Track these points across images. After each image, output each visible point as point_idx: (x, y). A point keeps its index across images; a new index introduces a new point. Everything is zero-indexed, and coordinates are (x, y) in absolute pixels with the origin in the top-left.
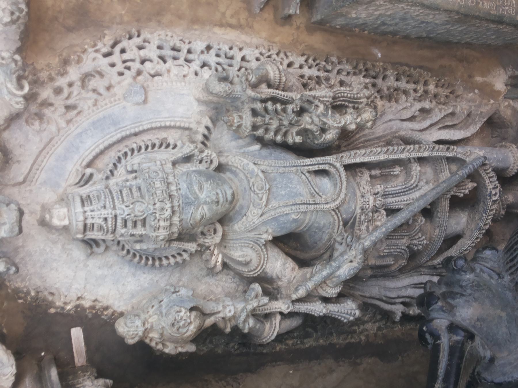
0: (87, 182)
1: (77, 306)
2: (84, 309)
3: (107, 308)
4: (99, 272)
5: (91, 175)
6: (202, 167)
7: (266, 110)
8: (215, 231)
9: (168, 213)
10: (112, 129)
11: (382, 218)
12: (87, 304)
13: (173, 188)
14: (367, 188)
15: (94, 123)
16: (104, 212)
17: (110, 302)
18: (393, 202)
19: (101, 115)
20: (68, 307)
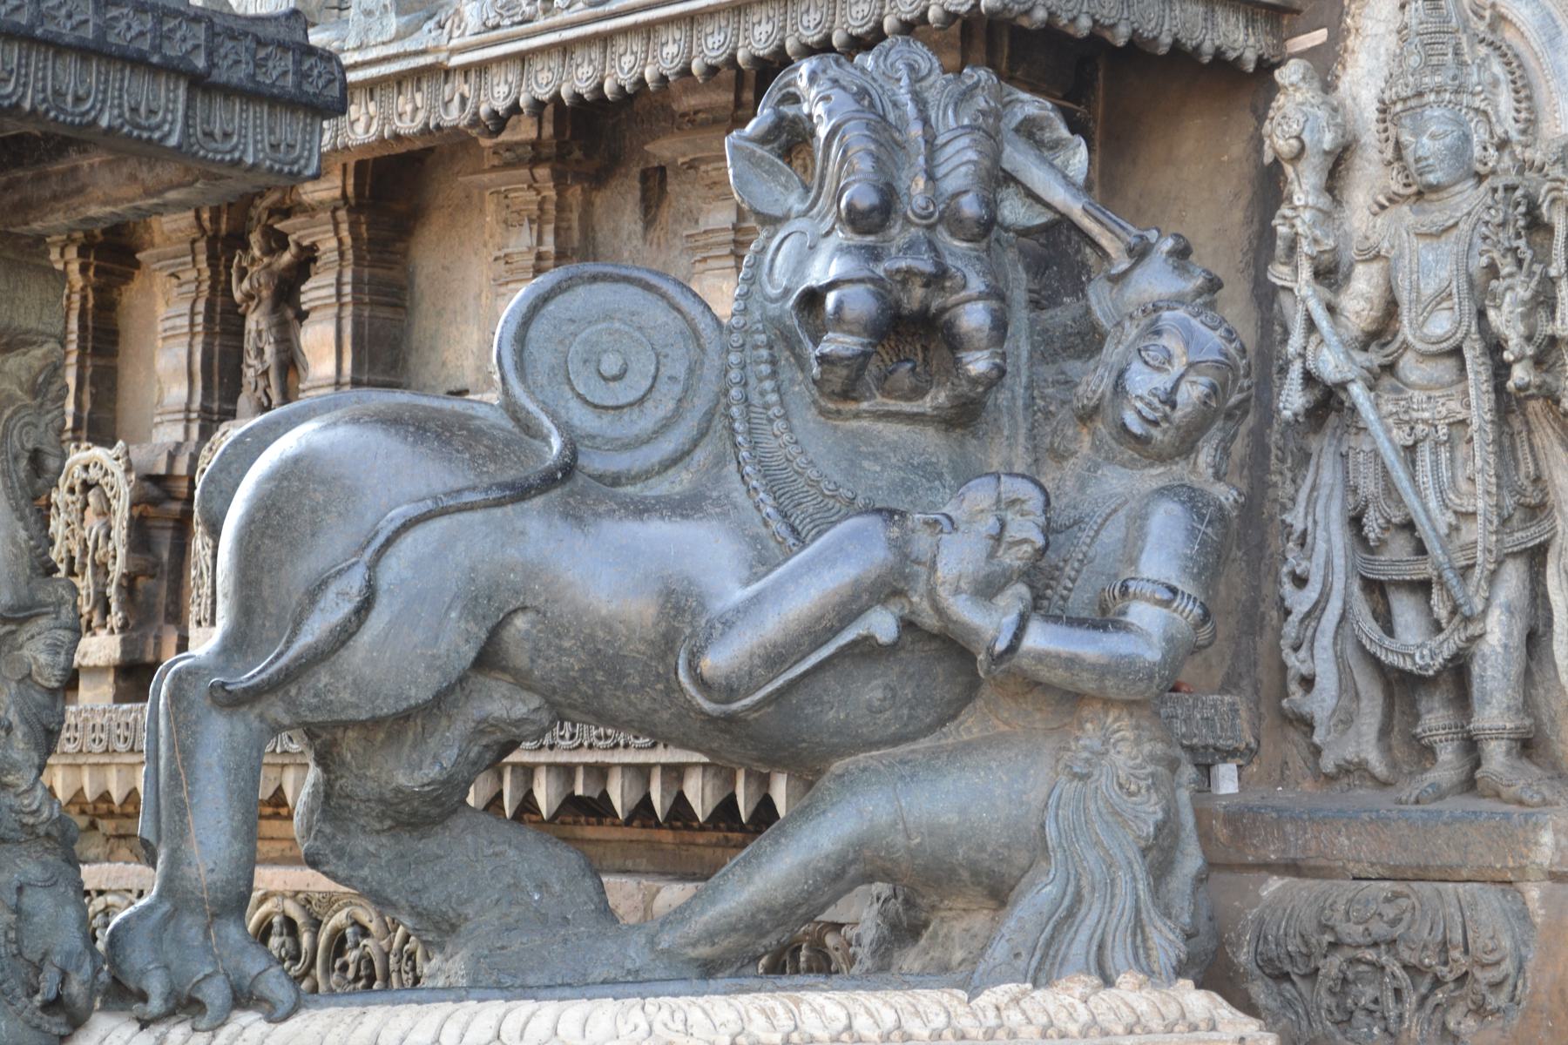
0: (1475, 13)
1: (1348, 30)
2: (1345, 39)
3: (1344, 68)
4: (1382, 50)
5: (1482, 18)
6: (1477, 151)
7: (1518, 204)
8: (1407, 185)
9: (1404, 94)
10: (1544, 39)
11: (1402, 436)
12: (1350, 42)
13: (1432, 97)
14: (1444, 412)
15: (1549, 14)
16: (1414, 21)
17: (1350, 71)
18: (1425, 455)
19: (1560, 22)
20: (1349, 20)
